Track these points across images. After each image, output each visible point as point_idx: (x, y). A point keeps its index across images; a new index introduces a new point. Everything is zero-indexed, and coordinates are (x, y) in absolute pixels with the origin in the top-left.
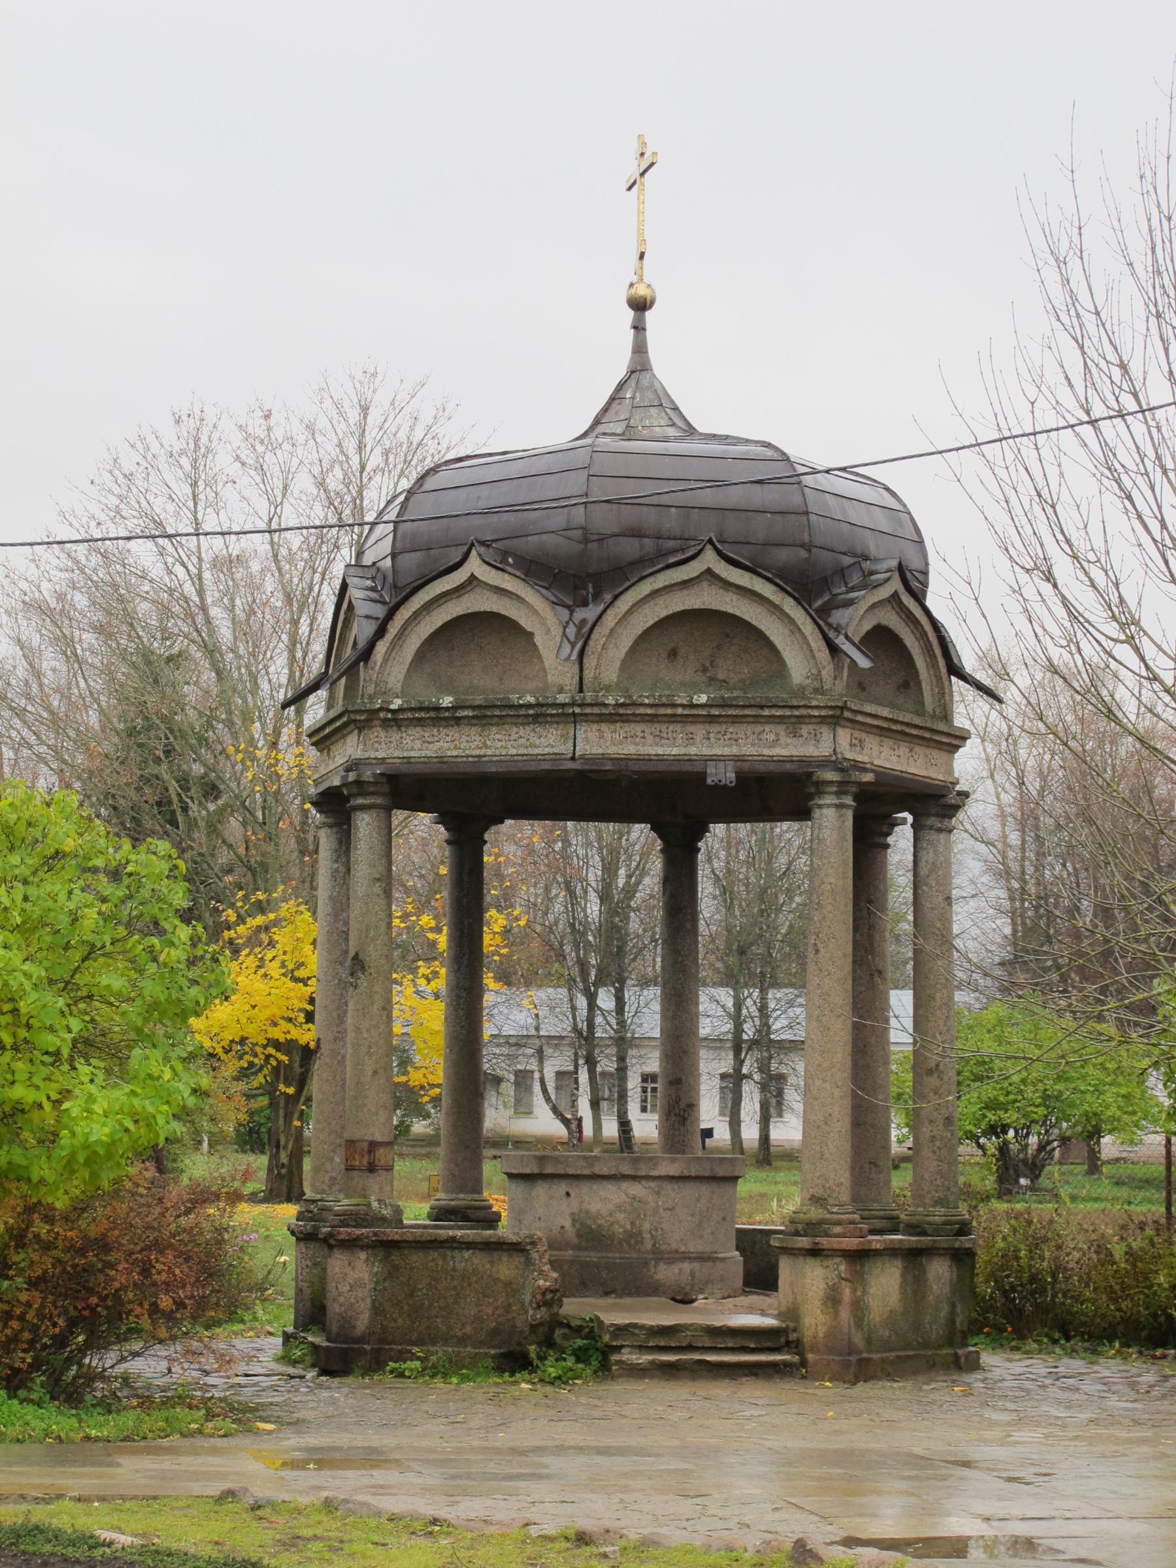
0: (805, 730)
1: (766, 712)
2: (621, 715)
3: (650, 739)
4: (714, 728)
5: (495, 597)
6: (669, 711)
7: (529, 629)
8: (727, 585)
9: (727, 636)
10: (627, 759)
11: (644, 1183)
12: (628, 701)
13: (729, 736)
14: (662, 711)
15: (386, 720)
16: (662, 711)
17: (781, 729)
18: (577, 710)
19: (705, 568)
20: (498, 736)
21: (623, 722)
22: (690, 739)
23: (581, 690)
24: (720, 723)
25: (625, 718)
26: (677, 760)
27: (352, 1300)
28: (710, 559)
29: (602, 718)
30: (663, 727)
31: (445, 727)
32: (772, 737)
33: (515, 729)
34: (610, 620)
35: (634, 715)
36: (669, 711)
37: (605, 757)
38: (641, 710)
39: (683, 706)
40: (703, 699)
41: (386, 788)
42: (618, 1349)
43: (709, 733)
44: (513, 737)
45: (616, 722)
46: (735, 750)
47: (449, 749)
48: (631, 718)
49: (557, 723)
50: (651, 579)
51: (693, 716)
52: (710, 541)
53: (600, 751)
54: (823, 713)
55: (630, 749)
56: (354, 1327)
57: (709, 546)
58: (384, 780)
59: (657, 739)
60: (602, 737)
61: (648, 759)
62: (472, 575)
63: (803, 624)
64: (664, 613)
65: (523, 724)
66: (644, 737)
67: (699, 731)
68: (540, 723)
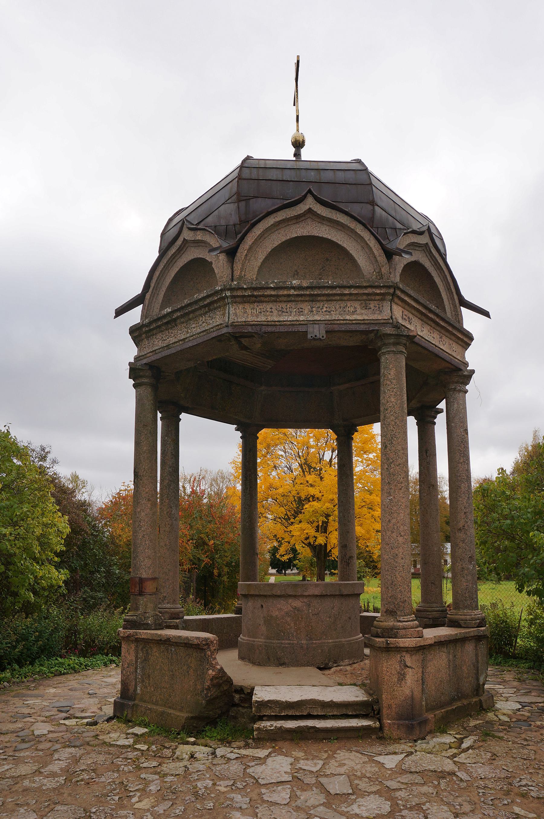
1: (347, 292)
3: (275, 312)
10: (260, 325)
13: (325, 309)
14: (281, 292)
15: (146, 332)
16: (281, 292)
20: (193, 326)
21: (258, 302)
22: (301, 312)
24: (319, 301)
25: (258, 299)
30: (284, 305)
31: (171, 328)
35: (263, 296)
36: (286, 292)
40: (305, 284)
44: (201, 323)
48: (262, 299)
53: (244, 319)
58: (148, 367)
59: (280, 313)
61: (273, 324)
66: (272, 312)
67: (306, 307)
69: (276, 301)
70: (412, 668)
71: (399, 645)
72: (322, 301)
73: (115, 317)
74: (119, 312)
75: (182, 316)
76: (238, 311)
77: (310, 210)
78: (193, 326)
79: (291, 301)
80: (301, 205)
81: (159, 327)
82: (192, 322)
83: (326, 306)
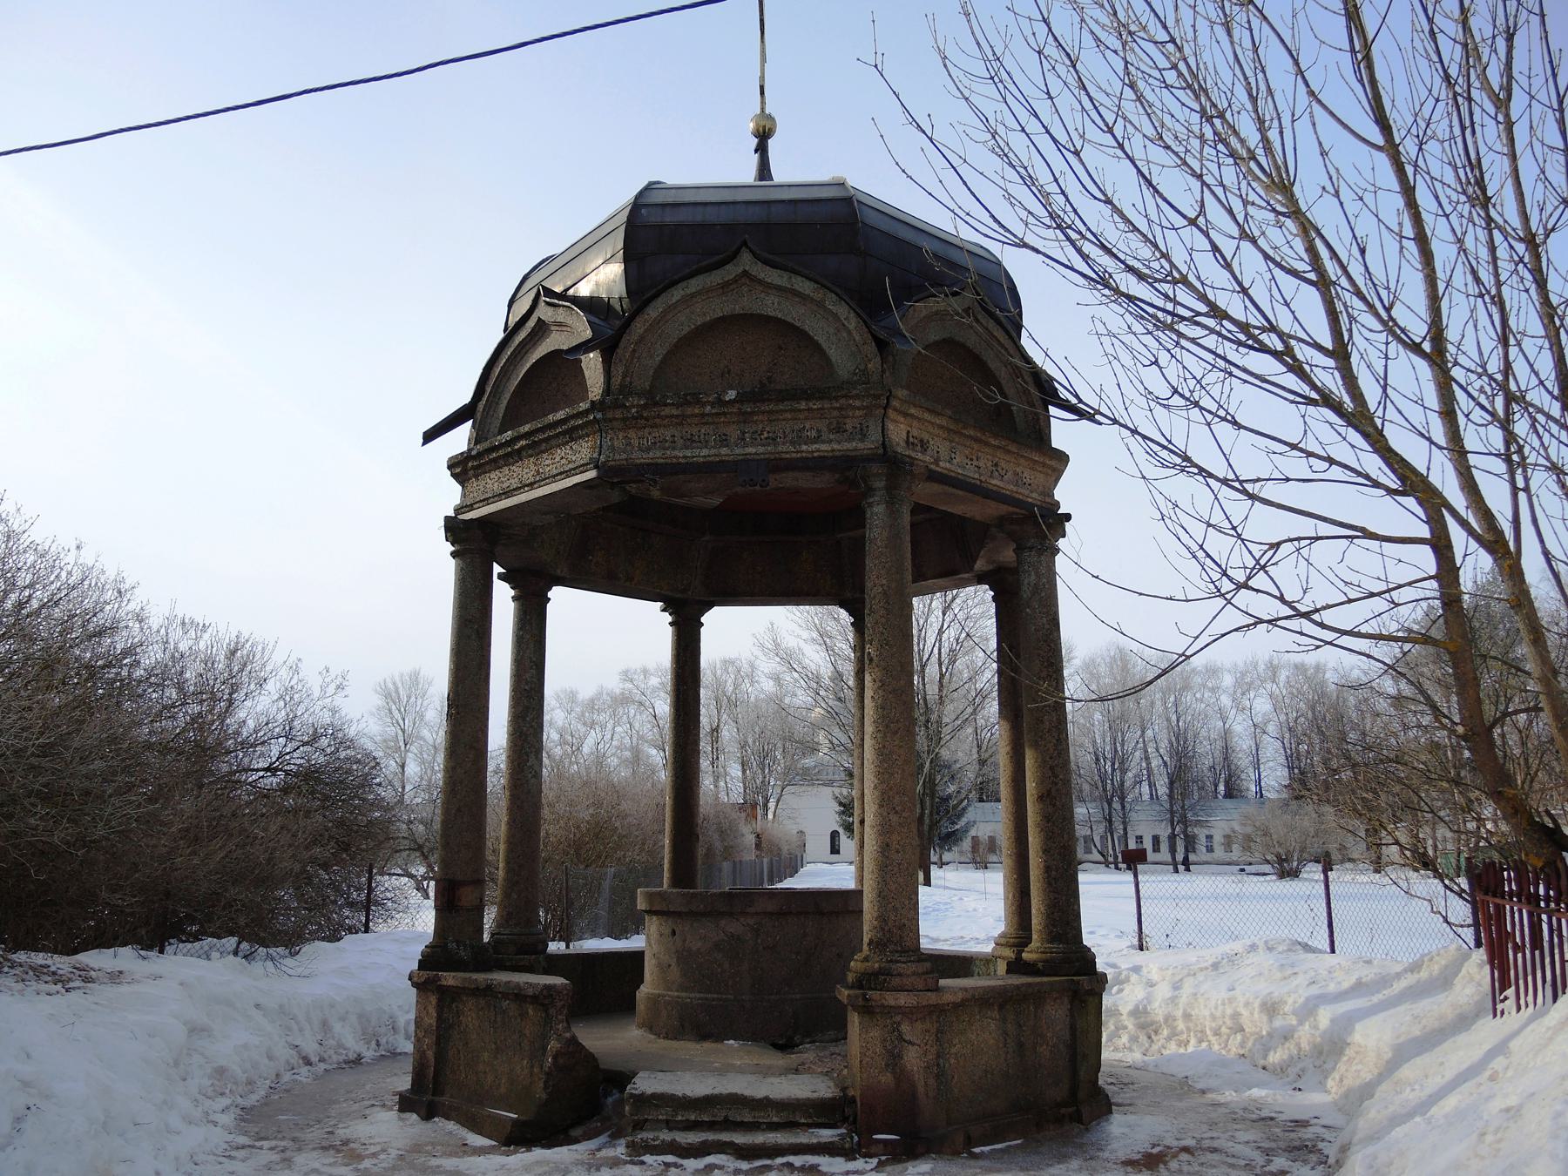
13: (766, 435)
20: (547, 462)
43: (744, 433)
50: (684, 284)
69: (681, 424)
70: (913, 1044)
71: (886, 1003)
73: (423, 444)
74: (430, 436)
78: (547, 462)
79: (706, 423)
81: (495, 460)
82: (545, 456)
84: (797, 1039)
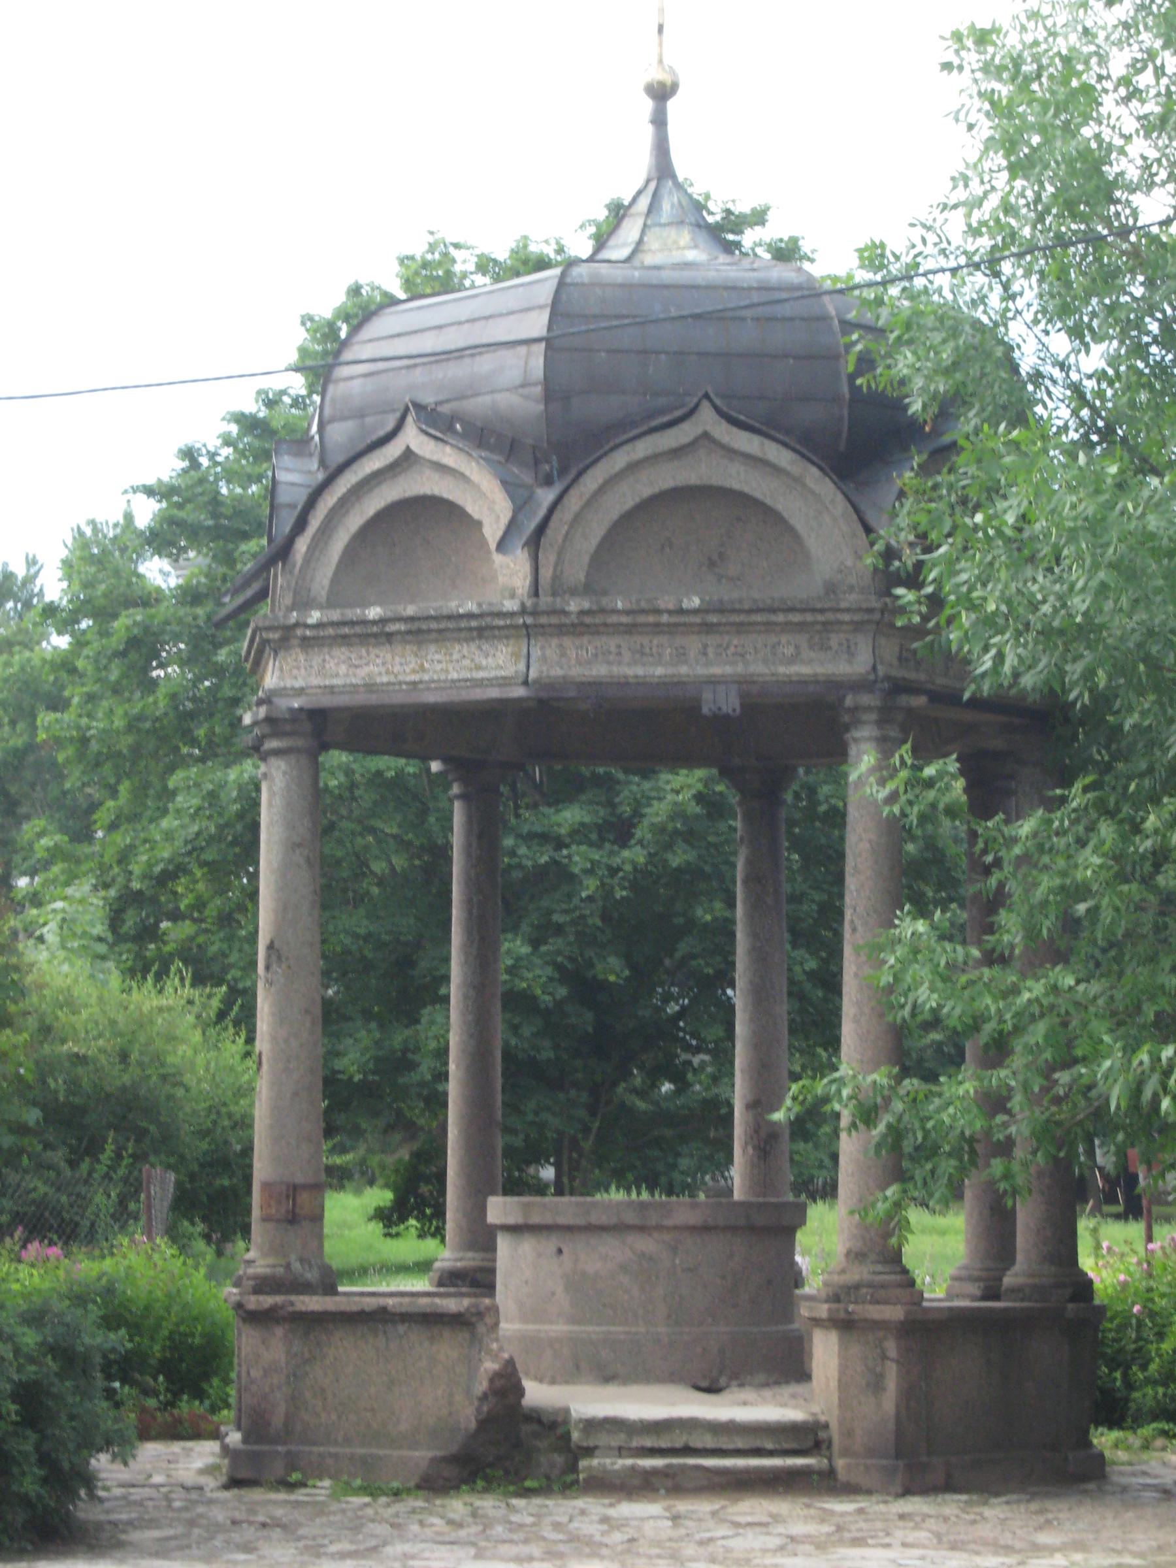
0: (834, 640)
2: (588, 626)
3: (627, 656)
4: (712, 640)
5: (436, 476)
6: (651, 619)
7: (476, 516)
8: (731, 453)
9: (739, 519)
11: (655, 1235)
12: (595, 607)
14: (642, 619)
15: (304, 639)
16: (642, 619)
17: (802, 639)
18: (529, 620)
19: (699, 431)
20: (437, 657)
21: (592, 634)
22: (681, 655)
23: (536, 593)
26: (665, 683)
27: (267, 1390)
28: (707, 420)
29: (562, 630)
30: (645, 640)
32: (789, 651)
33: (457, 647)
34: (574, 502)
36: (651, 619)
37: (566, 681)
38: (614, 619)
39: (670, 612)
40: (696, 602)
41: (307, 727)
42: (589, 1452)
44: (455, 656)
45: (581, 634)
46: (740, 669)
47: (380, 674)
48: (602, 629)
49: (507, 637)
51: (685, 624)
52: (707, 396)
54: (857, 617)
55: (600, 671)
56: (269, 1424)
57: (706, 404)
60: (563, 654)
61: (624, 684)
62: (408, 449)
63: (832, 501)
64: (647, 492)
65: (467, 640)
67: (693, 644)
68: (487, 639)
72: (728, 633)
75: (409, 632)
76: (548, 652)
77: (706, 435)
80: (685, 426)
81: (345, 637)
83: (735, 642)
84: (723, 1381)
